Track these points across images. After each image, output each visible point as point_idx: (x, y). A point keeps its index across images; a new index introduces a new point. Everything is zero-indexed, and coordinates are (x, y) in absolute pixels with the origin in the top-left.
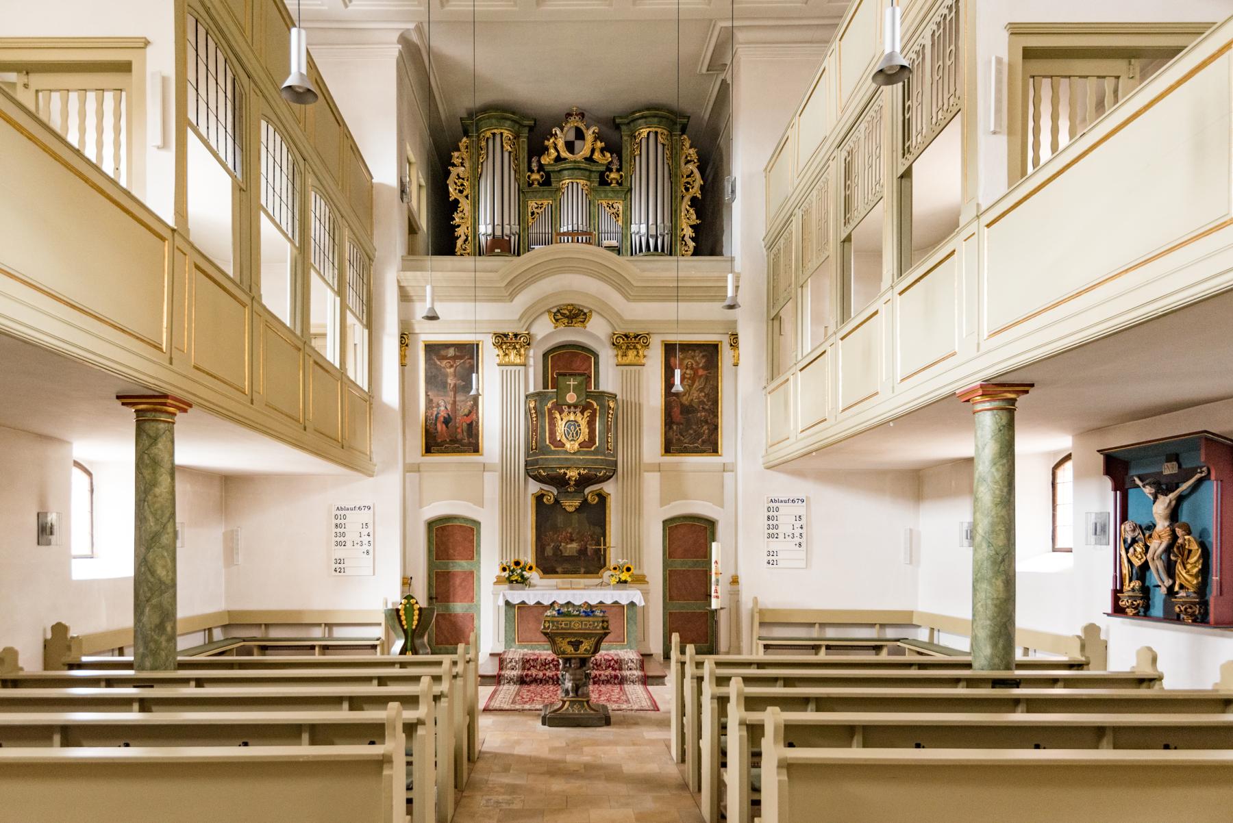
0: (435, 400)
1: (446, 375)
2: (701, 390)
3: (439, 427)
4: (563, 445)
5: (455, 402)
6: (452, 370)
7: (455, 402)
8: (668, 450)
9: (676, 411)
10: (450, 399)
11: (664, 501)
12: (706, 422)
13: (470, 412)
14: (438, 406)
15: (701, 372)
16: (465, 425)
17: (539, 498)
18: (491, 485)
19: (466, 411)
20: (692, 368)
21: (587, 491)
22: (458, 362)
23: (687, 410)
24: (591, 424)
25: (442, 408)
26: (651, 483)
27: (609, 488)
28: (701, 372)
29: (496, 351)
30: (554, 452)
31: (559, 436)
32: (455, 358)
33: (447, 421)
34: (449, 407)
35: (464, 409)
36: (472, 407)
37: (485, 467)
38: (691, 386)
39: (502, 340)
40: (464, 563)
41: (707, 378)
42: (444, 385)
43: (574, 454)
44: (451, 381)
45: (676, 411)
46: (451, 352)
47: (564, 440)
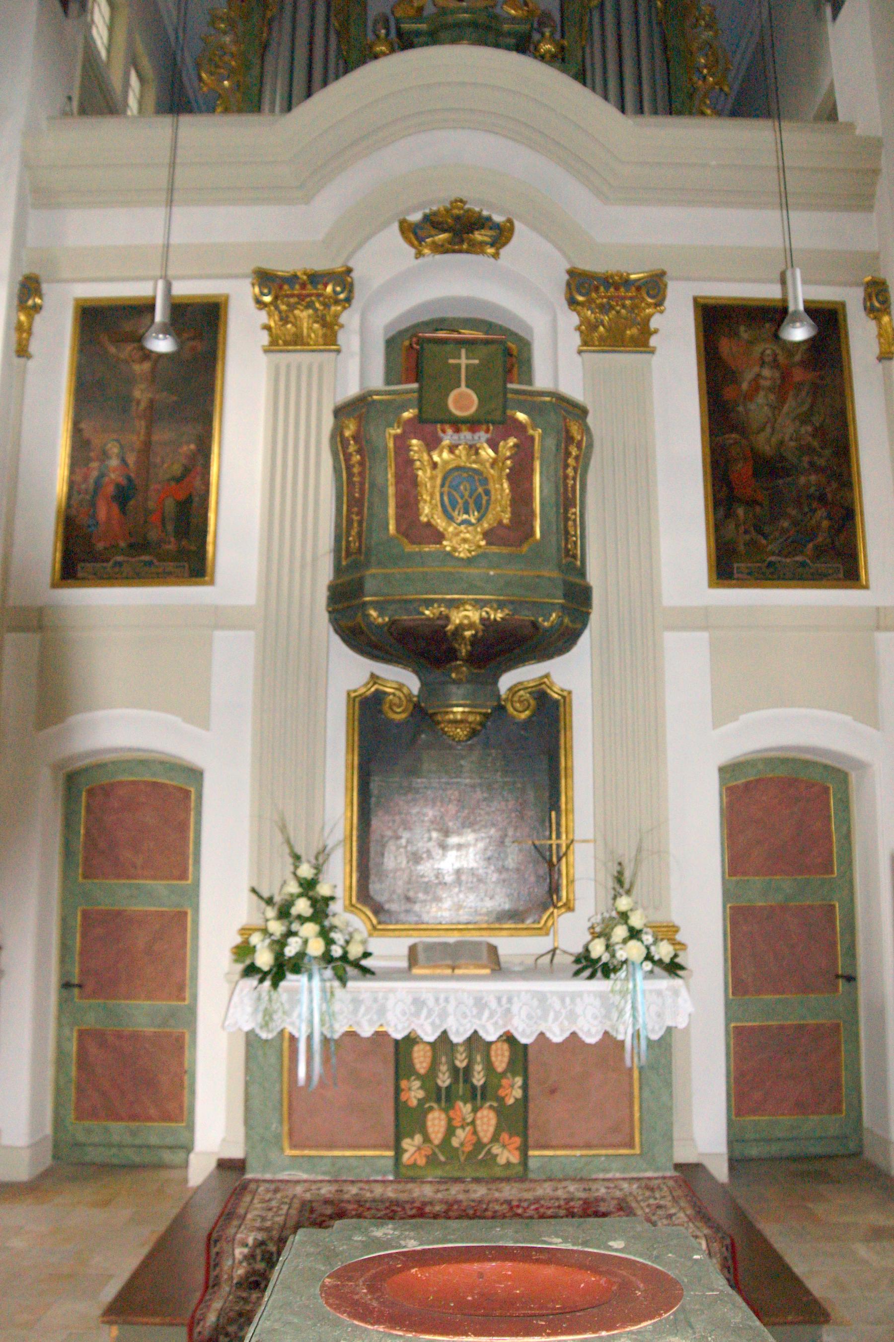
0: (96, 441)
1: (131, 381)
2: (805, 419)
3: (102, 513)
4: (439, 537)
7: (147, 446)
8: (727, 566)
9: (741, 469)
11: (723, 712)
12: (821, 498)
13: (187, 471)
14: (104, 455)
15: (798, 375)
16: (170, 505)
17: (368, 710)
18: (233, 665)
19: (177, 469)
20: (775, 364)
21: (507, 681)
23: (770, 468)
24: (520, 476)
25: (114, 462)
26: (686, 665)
27: (569, 672)
28: (798, 375)
29: (263, 317)
30: (411, 556)
31: (428, 511)
33: (123, 496)
34: (131, 459)
35: (169, 465)
36: (192, 458)
37: (222, 618)
38: (776, 408)
39: (281, 288)
40: (159, 886)
41: (816, 390)
42: (125, 403)
43: (469, 561)
45: (741, 469)
47: (440, 523)
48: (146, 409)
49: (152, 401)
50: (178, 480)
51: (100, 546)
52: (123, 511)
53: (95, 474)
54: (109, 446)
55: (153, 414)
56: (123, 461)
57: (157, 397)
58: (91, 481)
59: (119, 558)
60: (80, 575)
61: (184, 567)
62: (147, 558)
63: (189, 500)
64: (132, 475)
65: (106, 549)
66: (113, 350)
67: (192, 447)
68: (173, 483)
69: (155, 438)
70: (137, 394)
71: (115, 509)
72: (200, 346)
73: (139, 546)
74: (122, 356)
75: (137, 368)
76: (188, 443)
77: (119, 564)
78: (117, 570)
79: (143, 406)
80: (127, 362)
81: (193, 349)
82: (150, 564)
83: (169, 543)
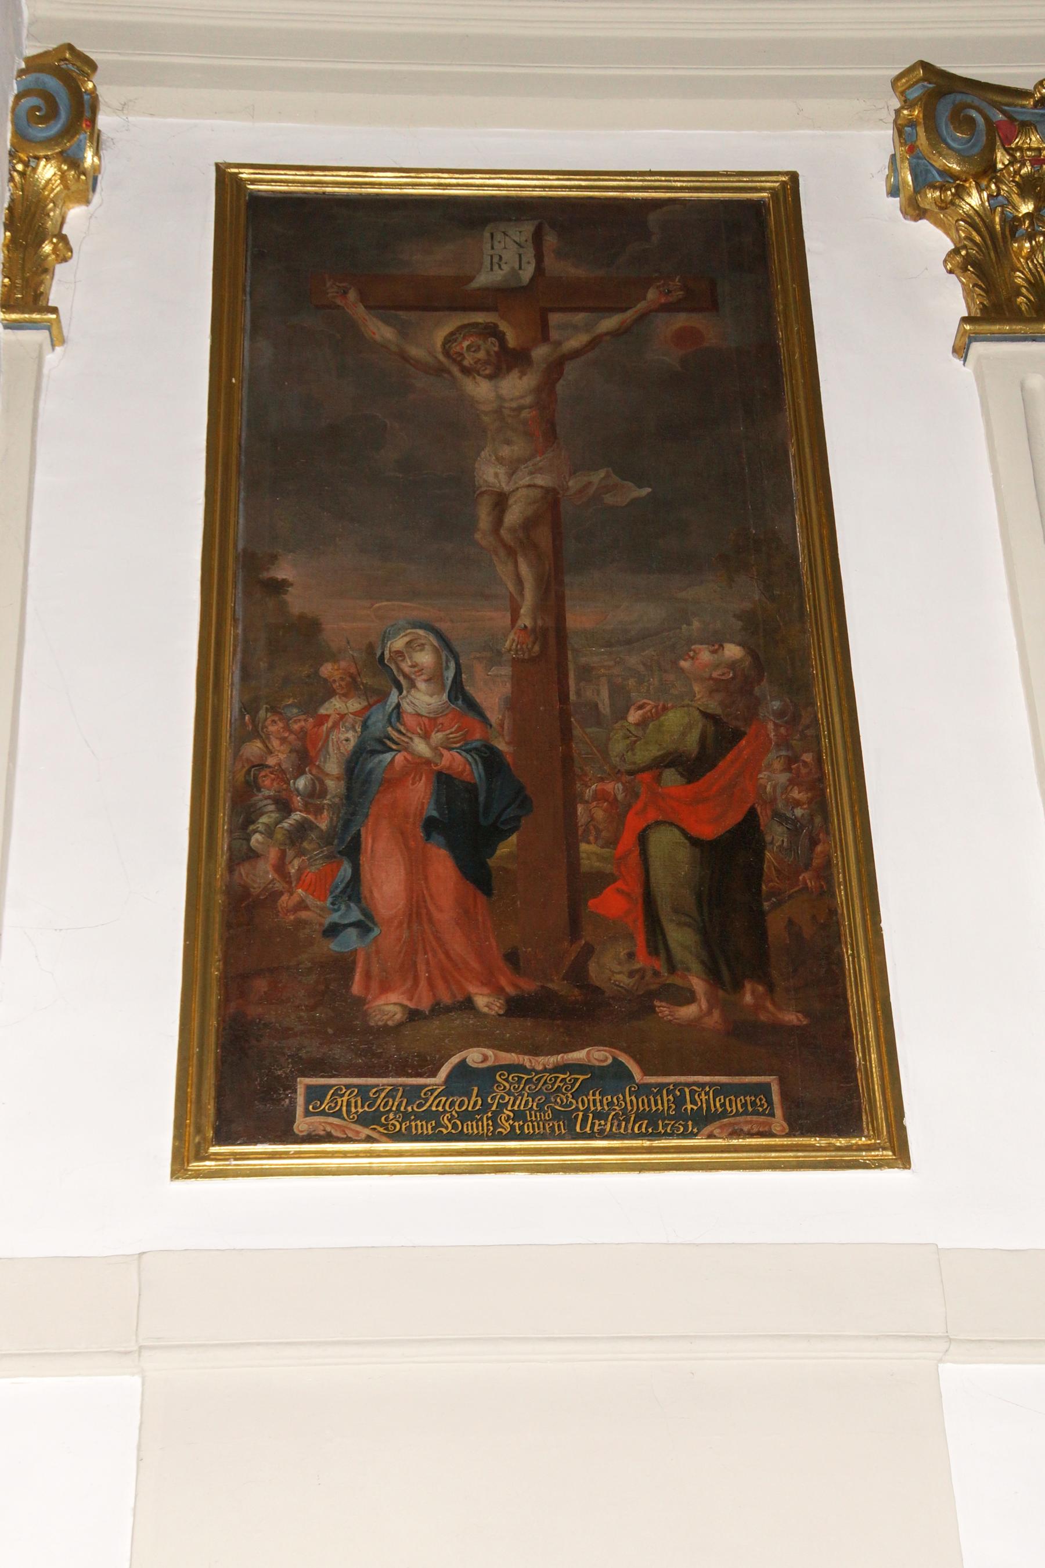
0: (346, 621)
1: (460, 429)
3: (387, 883)
5: (551, 645)
6: (516, 386)
7: (551, 645)
10: (501, 612)
13: (722, 736)
14: (378, 675)
19: (680, 728)
22: (573, 332)
25: (423, 699)
32: (536, 300)
33: (469, 822)
34: (492, 692)
36: (740, 687)
42: (438, 508)
44: (507, 473)
46: (505, 259)
48: (529, 525)
49: (551, 501)
50: (694, 766)
51: (389, 1007)
52: (477, 874)
53: (347, 739)
54: (399, 643)
55: (558, 543)
56: (458, 692)
57: (573, 484)
58: (333, 766)
59: (474, 1056)
60: (302, 1124)
61: (764, 1090)
62: (598, 1055)
63: (747, 835)
64: (501, 746)
65: (413, 1015)
66: (381, 331)
67: (733, 651)
68: (671, 777)
69: (580, 618)
70: (490, 473)
71: (442, 866)
72: (716, 331)
73: (556, 1007)
74: (414, 351)
75: (481, 389)
76: (716, 642)
77: (485, 1077)
78: (473, 1102)
79: (514, 515)
80: (440, 371)
81: (684, 336)
82: (618, 1074)
83: (688, 997)
